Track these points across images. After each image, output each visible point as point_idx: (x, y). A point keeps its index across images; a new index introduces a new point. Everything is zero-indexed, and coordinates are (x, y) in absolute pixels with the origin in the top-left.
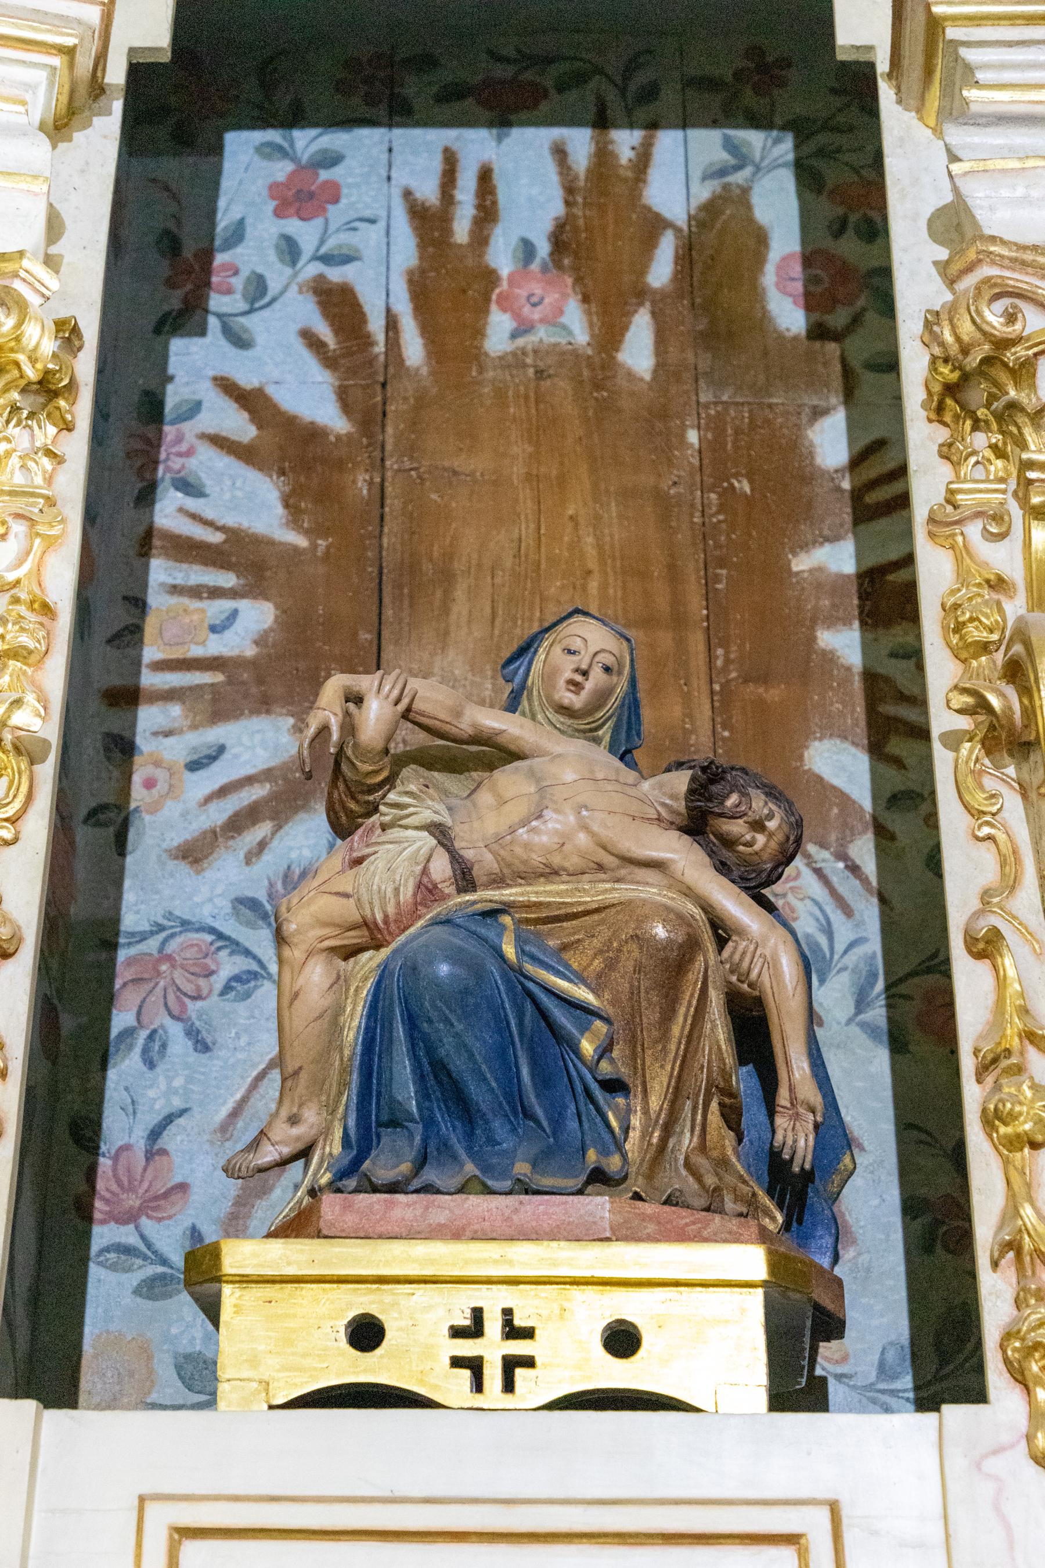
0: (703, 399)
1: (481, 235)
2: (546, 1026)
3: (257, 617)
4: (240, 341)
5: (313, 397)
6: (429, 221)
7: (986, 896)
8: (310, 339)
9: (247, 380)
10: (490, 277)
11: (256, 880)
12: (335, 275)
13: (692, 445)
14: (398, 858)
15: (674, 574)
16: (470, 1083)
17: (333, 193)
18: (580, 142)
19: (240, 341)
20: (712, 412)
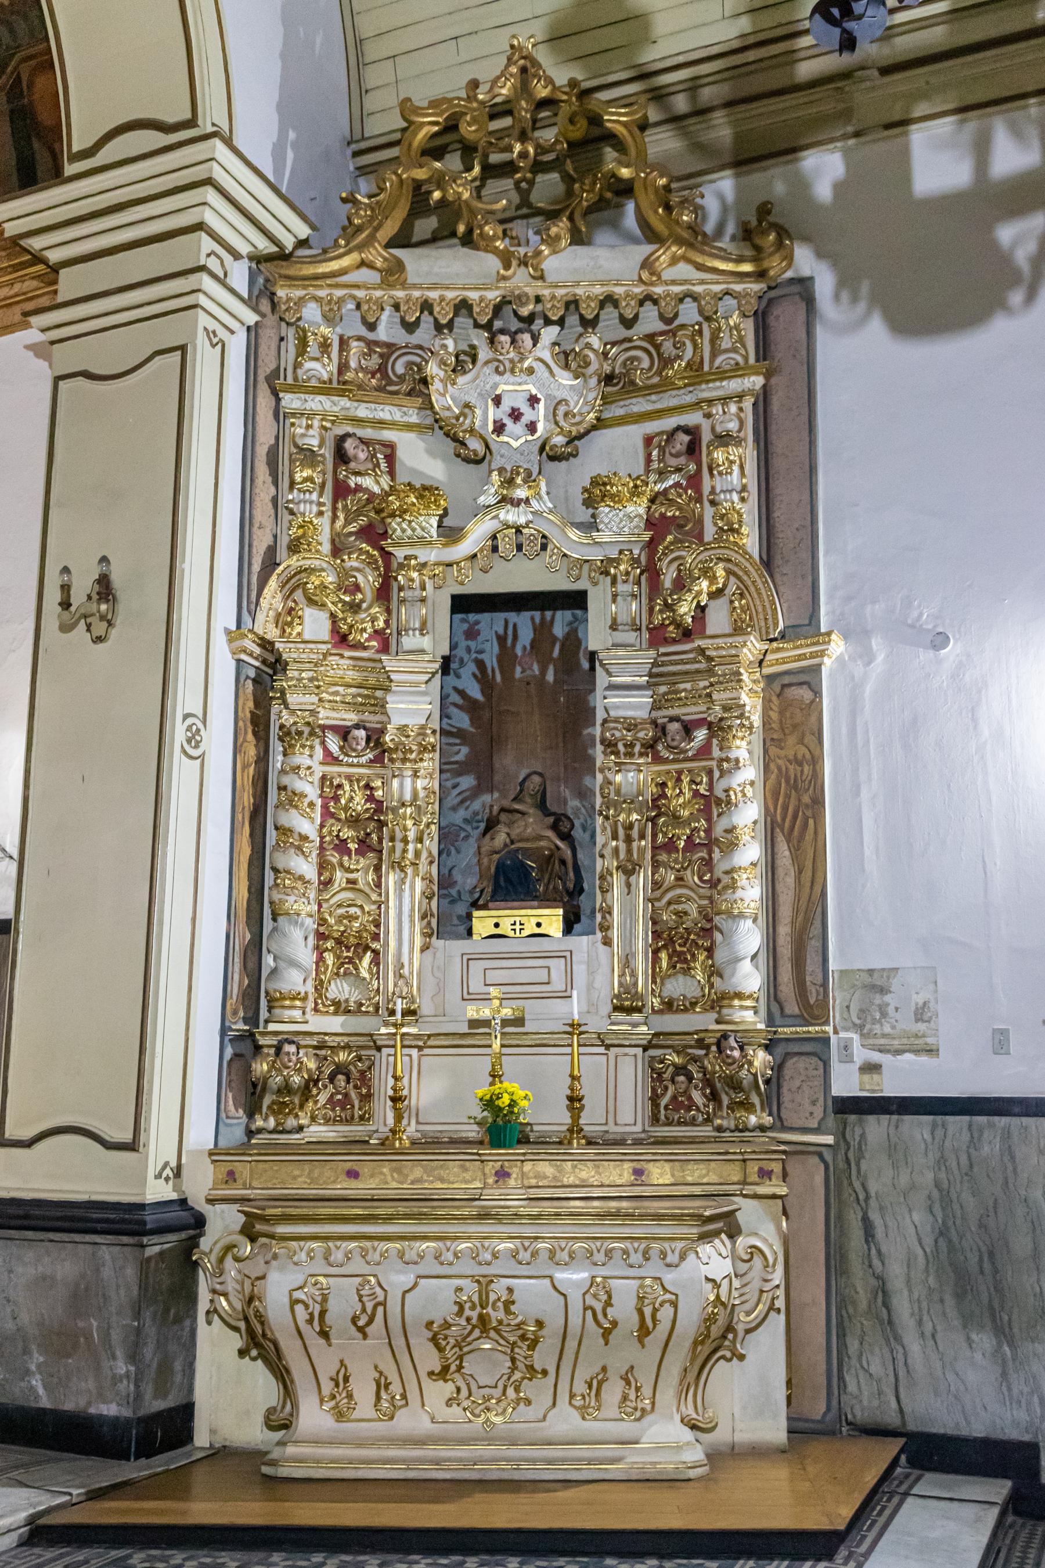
1: (514, 645)
2: (525, 871)
3: (465, 750)
4: (458, 676)
5: (475, 692)
6: (501, 639)
8: (474, 675)
9: (460, 687)
10: (516, 656)
11: (468, 814)
12: (480, 657)
14: (501, 838)
16: (512, 883)
17: (478, 633)
18: (537, 615)
19: (458, 676)
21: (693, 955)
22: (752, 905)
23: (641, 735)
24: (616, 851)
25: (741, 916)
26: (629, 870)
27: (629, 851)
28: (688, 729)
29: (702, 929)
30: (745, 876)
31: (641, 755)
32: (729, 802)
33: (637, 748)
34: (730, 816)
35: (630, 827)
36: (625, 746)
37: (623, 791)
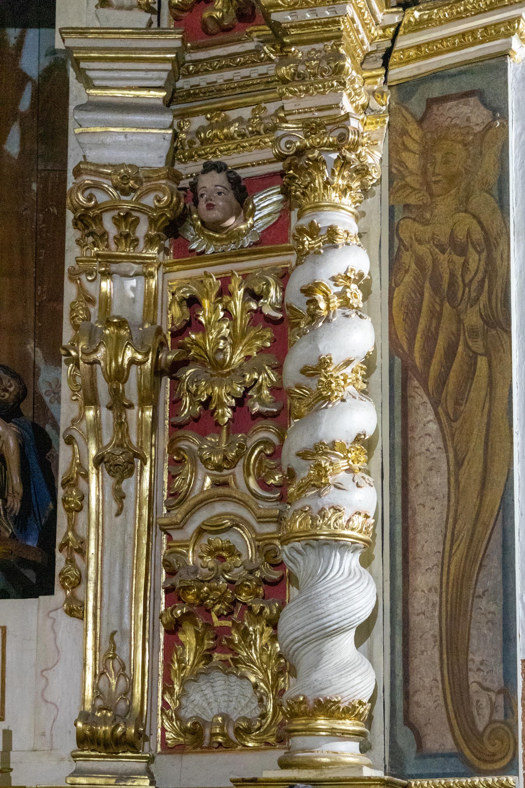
0: (39, 168)
7: (73, 421)
13: (34, 190)
15: (22, 251)
20: (43, 175)
21: (245, 634)
22: (358, 521)
23: (149, 200)
24: (96, 427)
25: (335, 543)
26: (119, 465)
27: (121, 425)
28: (242, 192)
29: (264, 581)
30: (343, 464)
31: (150, 241)
32: (314, 317)
33: (143, 229)
34: (314, 339)
35: (119, 376)
36: (117, 221)
37: (116, 310)
